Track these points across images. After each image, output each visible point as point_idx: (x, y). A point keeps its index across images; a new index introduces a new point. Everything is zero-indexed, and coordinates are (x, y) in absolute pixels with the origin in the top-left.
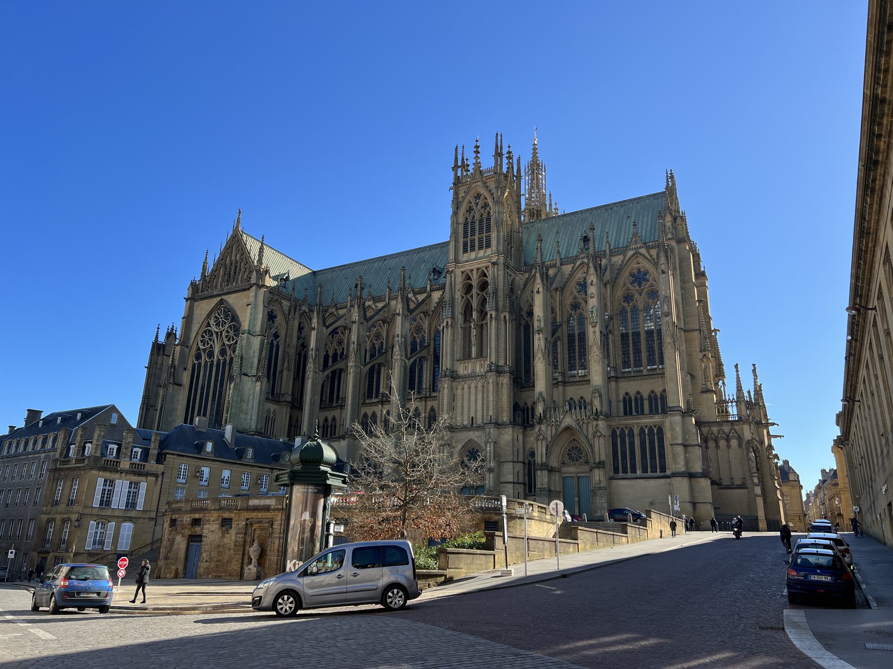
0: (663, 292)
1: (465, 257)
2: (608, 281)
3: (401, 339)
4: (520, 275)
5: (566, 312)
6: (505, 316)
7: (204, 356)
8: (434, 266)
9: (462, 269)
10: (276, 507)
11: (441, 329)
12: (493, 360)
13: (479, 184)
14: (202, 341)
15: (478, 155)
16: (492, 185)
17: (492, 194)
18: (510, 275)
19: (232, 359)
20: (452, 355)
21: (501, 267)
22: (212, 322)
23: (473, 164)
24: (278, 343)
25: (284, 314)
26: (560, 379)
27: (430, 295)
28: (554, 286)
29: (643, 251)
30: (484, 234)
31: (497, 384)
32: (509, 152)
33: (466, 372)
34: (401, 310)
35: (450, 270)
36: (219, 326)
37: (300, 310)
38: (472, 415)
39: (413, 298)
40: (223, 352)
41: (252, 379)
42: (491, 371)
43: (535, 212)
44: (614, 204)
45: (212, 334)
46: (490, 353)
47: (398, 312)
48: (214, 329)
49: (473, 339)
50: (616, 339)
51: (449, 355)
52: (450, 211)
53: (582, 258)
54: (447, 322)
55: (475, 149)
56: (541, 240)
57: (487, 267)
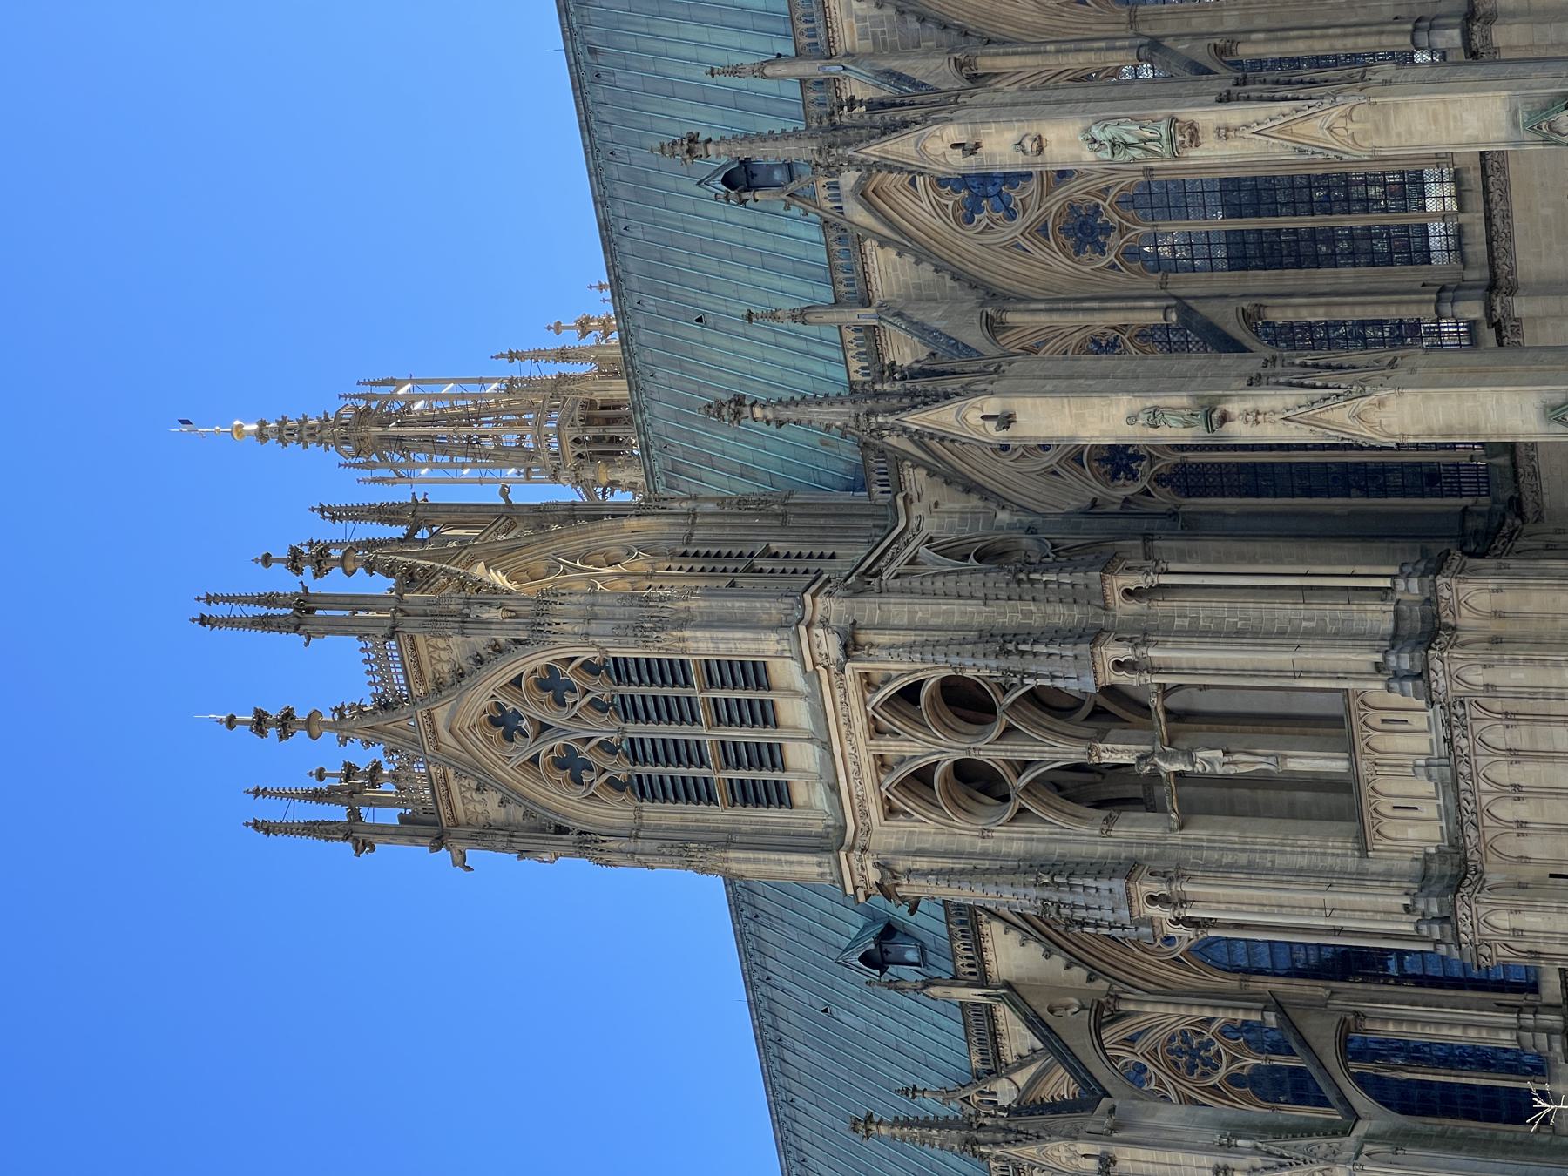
1: (810, 796)
2: (959, 65)
3: (1242, 1153)
4: (916, 510)
5: (1112, 275)
6: (1128, 593)
9: (875, 811)
11: (1190, 933)
12: (1364, 659)
13: (441, 714)
15: (301, 716)
16: (450, 650)
17: (498, 649)
18: (913, 561)
20: (1330, 878)
21: (869, 609)
23: (343, 741)
26: (1473, 310)
27: (1008, 985)
28: (974, 337)
30: (696, 693)
31: (1496, 641)
32: (295, 561)
33: (1430, 810)
34: (1083, 1147)
35: (874, 875)
39: (1022, 1077)
42: (1421, 675)
43: (593, 431)
44: (569, 36)
46: (1321, 674)
47: (1092, 1165)
49: (1246, 764)
50: (1260, 22)
51: (1330, 898)
52: (575, 868)
53: (837, 198)
54: (1152, 899)
55: (273, 732)
56: (739, 401)
57: (869, 683)
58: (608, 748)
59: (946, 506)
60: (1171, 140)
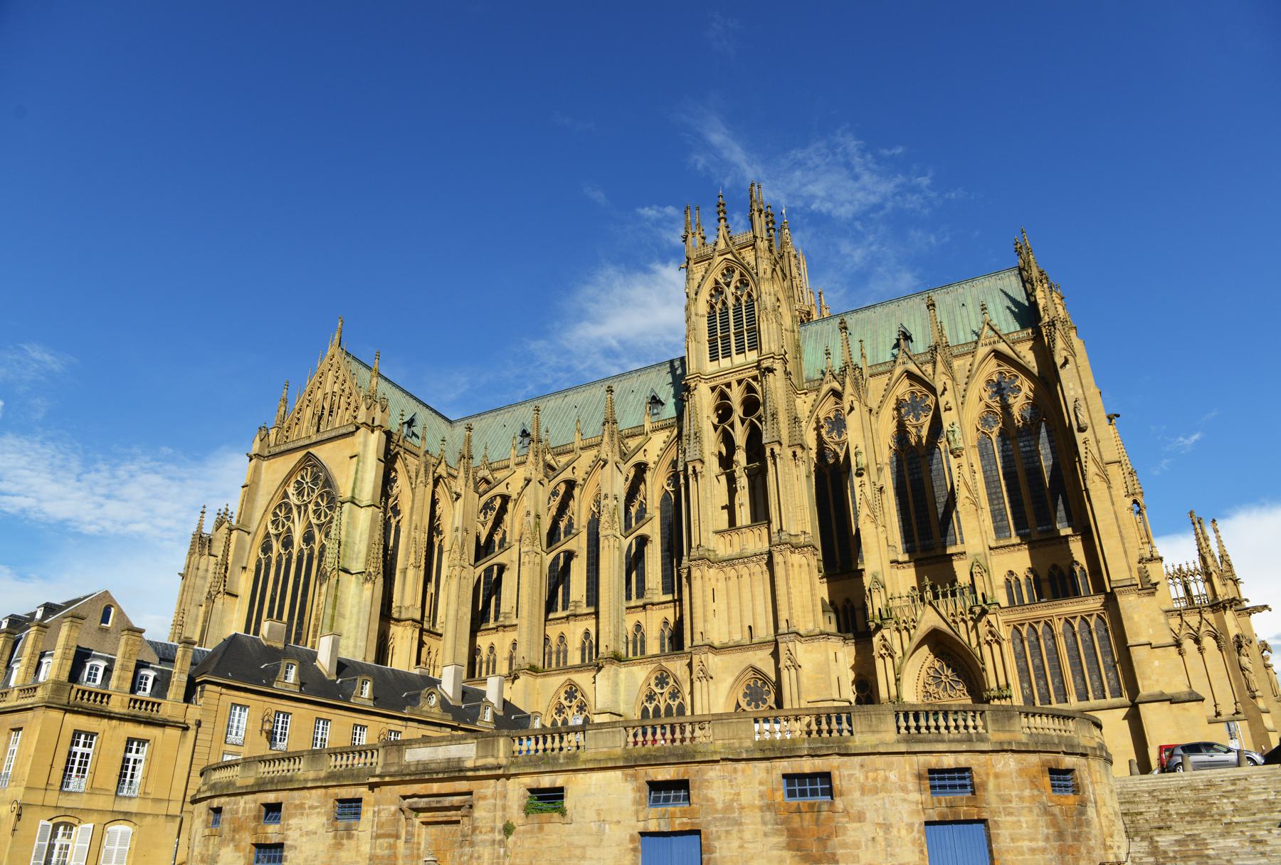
0: (1072, 393)
6: (794, 453)
7: (276, 546)
8: (653, 394)
9: (713, 384)
10: (480, 763)
14: (273, 522)
19: (323, 547)
22: (291, 490)
24: (398, 522)
25: (410, 478)
29: (1002, 347)
31: (792, 565)
36: (303, 496)
37: (434, 472)
38: (748, 622)
40: (309, 538)
41: (357, 578)
45: (291, 508)
48: (294, 500)
57: (755, 378)
58: (724, 303)
59: (805, 405)
60: (957, 449)
